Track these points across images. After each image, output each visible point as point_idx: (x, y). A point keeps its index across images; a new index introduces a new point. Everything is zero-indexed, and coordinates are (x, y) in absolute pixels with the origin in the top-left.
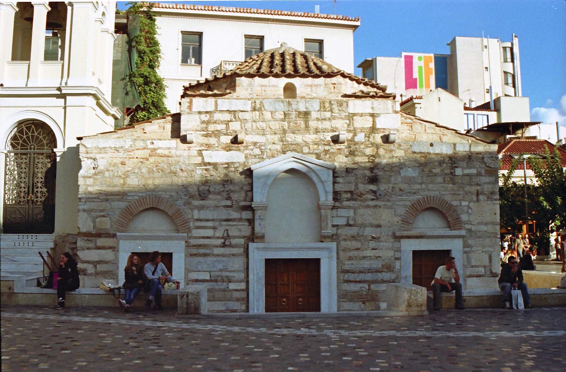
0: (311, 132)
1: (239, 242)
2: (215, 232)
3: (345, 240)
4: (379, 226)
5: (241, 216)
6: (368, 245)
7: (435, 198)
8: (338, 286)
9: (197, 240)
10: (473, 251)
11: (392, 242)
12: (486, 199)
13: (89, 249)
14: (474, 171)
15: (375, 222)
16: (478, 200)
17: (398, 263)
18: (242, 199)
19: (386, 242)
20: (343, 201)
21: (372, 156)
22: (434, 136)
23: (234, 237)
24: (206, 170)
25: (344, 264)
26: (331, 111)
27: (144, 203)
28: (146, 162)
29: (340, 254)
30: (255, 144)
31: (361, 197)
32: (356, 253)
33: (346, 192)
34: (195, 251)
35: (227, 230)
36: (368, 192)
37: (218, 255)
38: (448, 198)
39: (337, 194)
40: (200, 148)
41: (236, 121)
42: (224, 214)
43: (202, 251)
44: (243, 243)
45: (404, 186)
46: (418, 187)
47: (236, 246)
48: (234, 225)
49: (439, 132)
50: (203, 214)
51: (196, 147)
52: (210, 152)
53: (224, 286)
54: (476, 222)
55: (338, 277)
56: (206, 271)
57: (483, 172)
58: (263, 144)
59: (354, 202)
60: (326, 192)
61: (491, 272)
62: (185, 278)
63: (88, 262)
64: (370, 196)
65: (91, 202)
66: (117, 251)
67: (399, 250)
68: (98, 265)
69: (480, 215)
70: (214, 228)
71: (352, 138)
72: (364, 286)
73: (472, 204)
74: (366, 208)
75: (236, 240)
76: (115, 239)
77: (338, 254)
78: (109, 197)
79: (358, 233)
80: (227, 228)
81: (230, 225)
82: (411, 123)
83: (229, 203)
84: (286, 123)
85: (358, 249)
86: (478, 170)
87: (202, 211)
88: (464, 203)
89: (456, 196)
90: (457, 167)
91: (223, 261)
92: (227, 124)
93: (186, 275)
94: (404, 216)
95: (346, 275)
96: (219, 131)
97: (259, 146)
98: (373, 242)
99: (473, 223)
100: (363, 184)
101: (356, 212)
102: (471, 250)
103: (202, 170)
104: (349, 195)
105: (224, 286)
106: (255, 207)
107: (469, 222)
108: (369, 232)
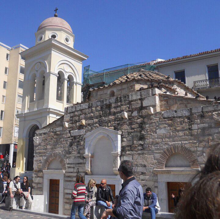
2: (74, 169)
21: (141, 123)
23: (81, 172)
24: (72, 139)
26: (121, 101)
34: (67, 179)
43: (70, 179)
57: (213, 125)
63: (35, 183)
64: (140, 148)
67: (156, 181)
70: (74, 168)
80: (78, 167)
82: (167, 100)
90: (193, 124)
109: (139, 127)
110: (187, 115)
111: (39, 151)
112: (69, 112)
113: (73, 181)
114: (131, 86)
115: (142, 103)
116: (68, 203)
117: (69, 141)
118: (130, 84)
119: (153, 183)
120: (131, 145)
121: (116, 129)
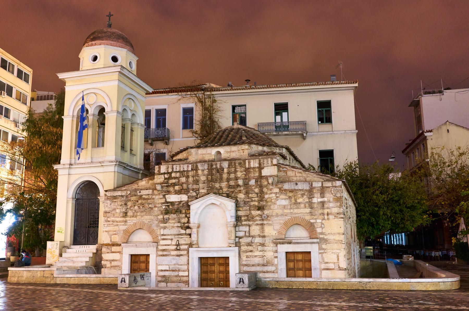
0: (224, 181)
4: (264, 237)
6: (257, 249)
7: (299, 218)
10: (326, 253)
11: (272, 247)
12: (334, 217)
13: (108, 253)
14: (325, 199)
15: (261, 235)
16: (328, 219)
17: (276, 259)
18: (186, 222)
19: (268, 246)
20: (243, 221)
22: (301, 178)
23: (182, 245)
28: (137, 203)
29: (241, 254)
30: (193, 190)
31: (253, 218)
34: (161, 253)
35: (178, 240)
36: (257, 215)
37: (173, 255)
38: (308, 218)
39: (239, 217)
40: (164, 194)
41: (183, 177)
42: (175, 231)
43: (165, 253)
45: (280, 212)
46: (288, 211)
47: (184, 250)
48: (182, 238)
49: (304, 175)
50: (166, 232)
51: (163, 193)
53: (176, 273)
54: (327, 233)
57: (331, 200)
61: (339, 267)
62: (156, 269)
63: (107, 260)
64: (258, 218)
65: (109, 226)
66: (122, 254)
67: (276, 251)
68: (112, 263)
69: (330, 228)
70: (172, 239)
73: (324, 222)
74: (256, 225)
76: (121, 247)
78: (118, 223)
83: (179, 225)
85: (251, 251)
86: (328, 199)
88: (319, 221)
89: (313, 216)
90: (314, 197)
91: (176, 259)
92: (179, 179)
93: (157, 267)
94: (279, 230)
99: (325, 234)
101: (250, 228)
102: (324, 252)
103: (166, 206)
104: (246, 218)
105: (176, 273)
107: (322, 233)
108: (258, 240)
109: (257, 197)
110: (308, 189)
111: (113, 219)
113: (172, 255)
114: (242, 150)
116: (163, 282)
117: (164, 207)
118: (241, 147)
119: (272, 253)
121: (230, 197)
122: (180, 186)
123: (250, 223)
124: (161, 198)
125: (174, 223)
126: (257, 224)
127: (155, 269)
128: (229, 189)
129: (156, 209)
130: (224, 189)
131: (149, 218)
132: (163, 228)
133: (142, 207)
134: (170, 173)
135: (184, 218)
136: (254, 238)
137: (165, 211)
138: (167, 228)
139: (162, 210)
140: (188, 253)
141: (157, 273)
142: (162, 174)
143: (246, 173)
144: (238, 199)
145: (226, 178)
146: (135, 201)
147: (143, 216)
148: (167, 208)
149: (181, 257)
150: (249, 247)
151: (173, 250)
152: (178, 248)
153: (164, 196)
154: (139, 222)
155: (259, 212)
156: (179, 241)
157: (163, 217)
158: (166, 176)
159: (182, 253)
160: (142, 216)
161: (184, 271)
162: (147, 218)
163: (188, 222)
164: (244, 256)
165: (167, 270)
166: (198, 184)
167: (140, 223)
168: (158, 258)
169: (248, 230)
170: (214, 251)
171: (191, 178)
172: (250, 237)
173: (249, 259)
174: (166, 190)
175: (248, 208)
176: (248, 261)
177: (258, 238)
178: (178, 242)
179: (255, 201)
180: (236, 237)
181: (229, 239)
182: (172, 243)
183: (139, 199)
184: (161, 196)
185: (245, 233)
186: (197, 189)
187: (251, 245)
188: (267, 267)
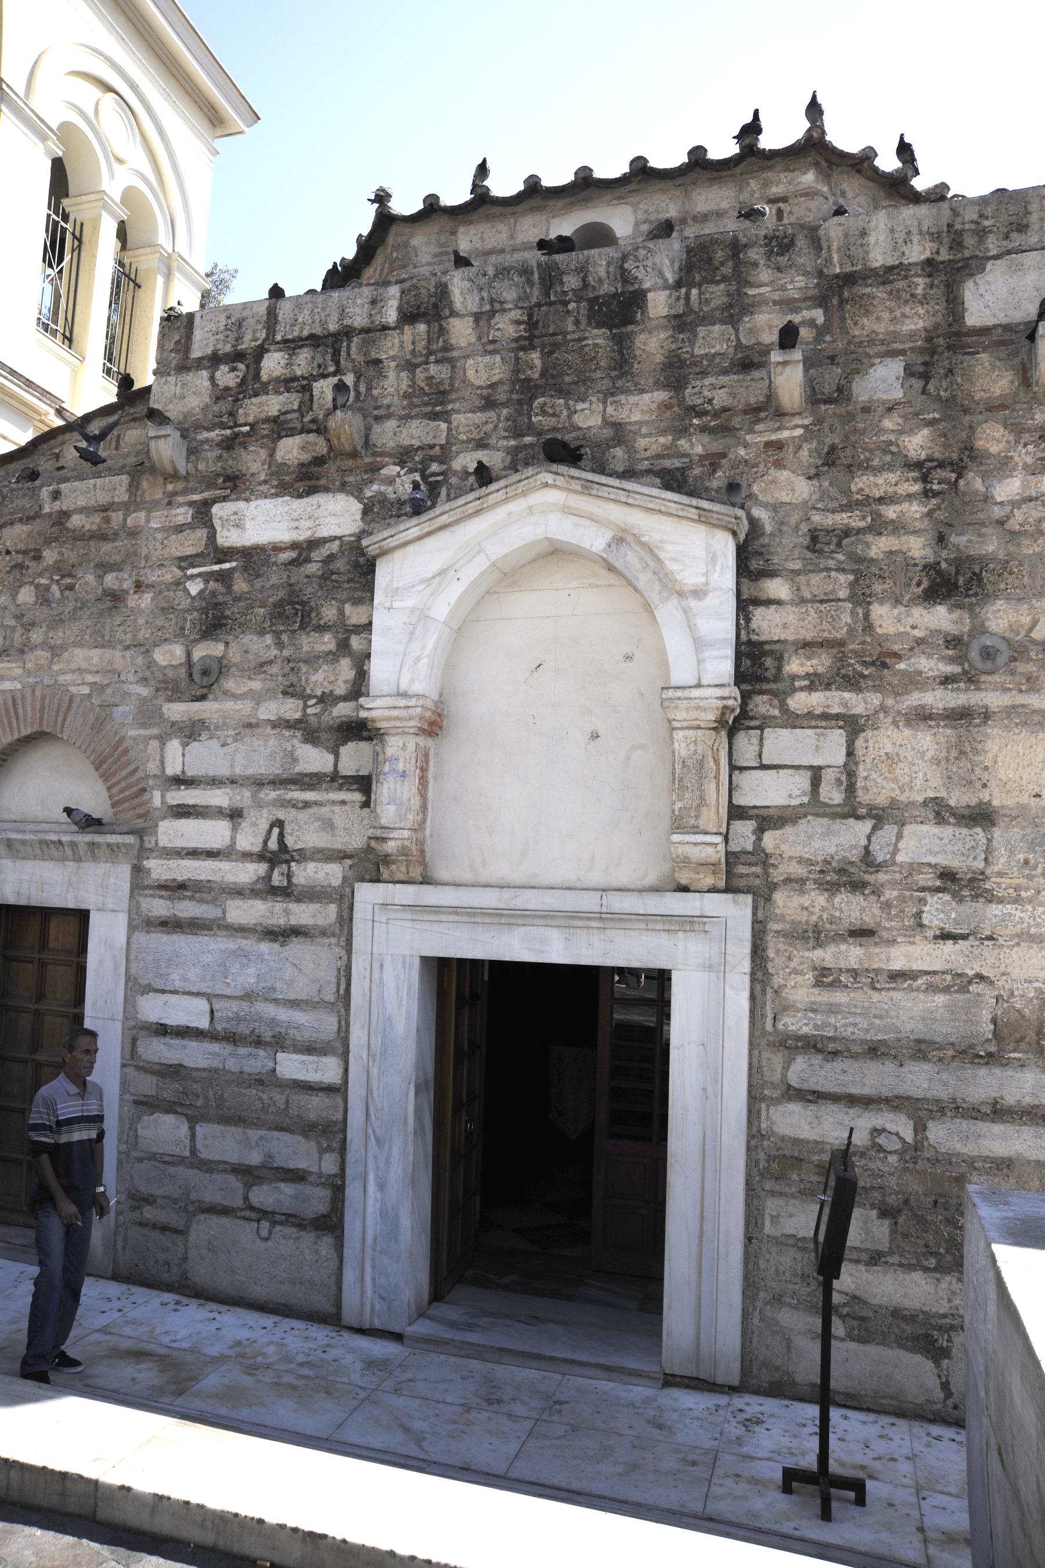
0: (645, 381)
1: (321, 875)
2: (235, 829)
3: (798, 884)
5: (336, 766)
6: (919, 915)
8: (753, 1114)
9: (173, 863)
15: (958, 798)
18: (341, 690)
19: (1017, 900)
20: (794, 690)
24: (223, 577)
25: (788, 1007)
27: (17, 718)
28: (32, 564)
29: (771, 952)
30: (403, 456)
31: (884, 665)
32: (853, 954)
33: (807, 646)
34: (159, 907)
35: (280, 824)
36: (920, 642)
37: (241, 930)
39: (764, 654)
40: (206, 495)
43: (187, 909)
44: (336, 882)
47: (313, 894)
48: (307, 805)
51: (193, 491)
52: (242, 504)
53: (256, 1062)
55: (754, 1070)
56: (198, 994)
58: (437, 451)
59: (846, 695)
60: (699, 644)
62: (126, 1018)
64: (930, 665)
70: (235, 815)
71: (840, 390)
72: (891, 1127)
74: (908, 723)
75: (311, 866)
77: (758, 953)
79: (866, 848)
81: (293, 804)
83: (291, 709)
84: (535, 357)
85: (862, 933)
87: (195, 745)
91: (260, 956)
92: (307, 389)
93: (129, 1002)
95: (800, 1064)
96: (274, 420)
97: (422, 462)
98: (947, 897)
100: (897, 602)
101: (859, 743)
103: (207, 577)
104: (821, 663)
105: (256, 1062)
106: (389, 719)
109: (927, 494)
112: (196, 354)
113: (228, 927)
115: (954, 305)
116: (170, 1108)
117: (194, 588)
118: (766, 184)
120: (841, 634)
122: (312, 437)
123: (857, 703)
124: (180, 529)
125: (258, 698)
126: (922, 717)
127: (121, 1017)
128: (684, 444)
129: (146, 600)
130: (642, 443)
131: (96, 660)
132: (181, 729)
133: (58, 594)
134: (260, 352)
135: (332, 657)
136: (889, 832)
137: (204, 611)
138: (204, 735)
139: (185, 603)
140: (346, 920)
141: (134, 1040)
142: (199, 362)
143: (828, 318)
144: (757, 512)
145: (659, 358)
146: (25, 553)
147: (63, 648)
148: (214, 594)
149: (296, 948)
150: (842, 899)
151: (238, 892)
152: (277, 879)
153: (203, 513)
154: (38, 693)
155: (941, 610)
156: (288, 829)
157: (189, 655)
158: (226, 377)
159: (303, 914)
160: (55, 651)
161: (310, 1049)
162: (84, 665)
163: (359, 687)
164: (796, 972)
165: (197, 1034)
166: (444, 416)
167: (43, 697)
168: (142, 938)
169: (840, 758)
170: (547, 917)
171: (392, 375)
172: (858, 818)
173: (840, 997)
174: (218, 467)
175: (844, 579)
176: (833, 1009)
177: (931, 830)
178: (281, 835)
179: (898, 527)
180: (737, 813)
181: (679, 824)
182: (233, 843)
183: (48, 541)
184: (183, 514)
185: (816, 782)
186: (432, 447)
187: (857, 886)
188: (997, 1071)
